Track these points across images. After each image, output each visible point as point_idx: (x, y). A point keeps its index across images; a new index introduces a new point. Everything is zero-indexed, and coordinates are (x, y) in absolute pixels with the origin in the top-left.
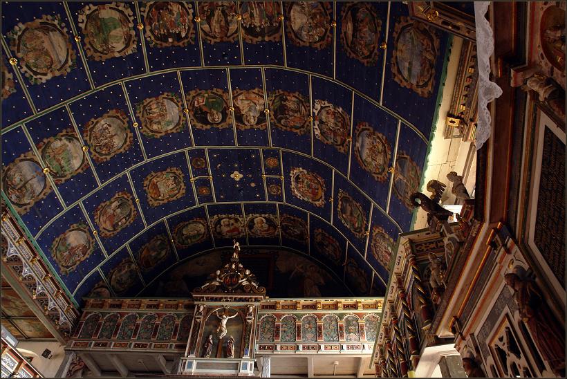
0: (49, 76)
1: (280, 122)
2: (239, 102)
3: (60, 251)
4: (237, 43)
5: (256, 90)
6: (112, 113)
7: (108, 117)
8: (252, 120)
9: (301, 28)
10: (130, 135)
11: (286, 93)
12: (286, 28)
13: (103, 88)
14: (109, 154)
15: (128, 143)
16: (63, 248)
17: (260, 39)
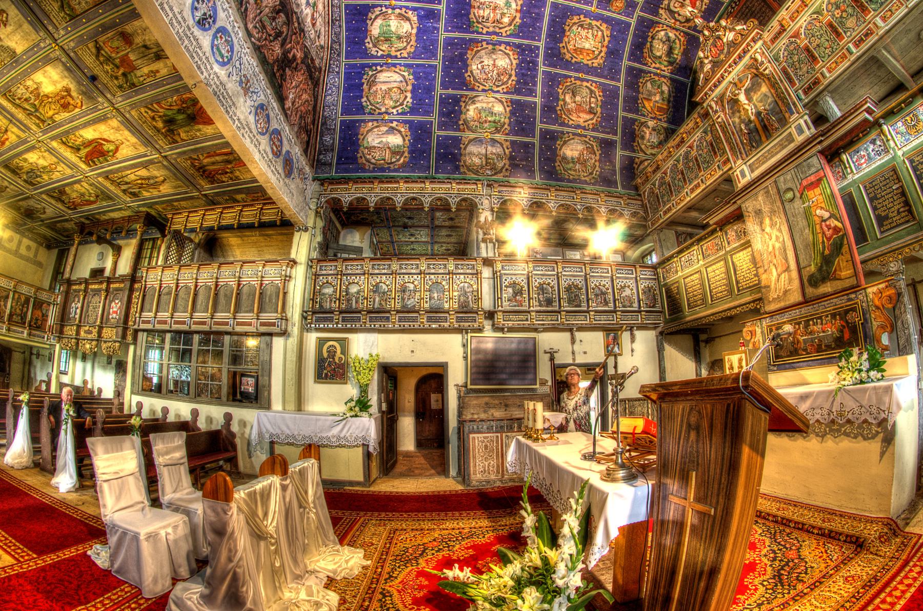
0: (409, 95)
6: (470, 54)
7: (472, 59)
10: (502, 47)
13: (440, 53)
14: (510, 76)
15: (511, 53)
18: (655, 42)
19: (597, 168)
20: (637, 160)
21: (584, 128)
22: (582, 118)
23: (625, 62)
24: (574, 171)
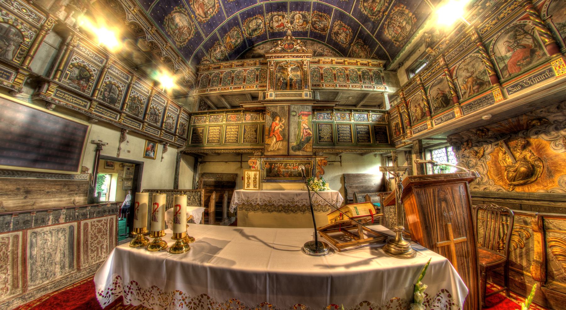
3: (172, 29)
16: (173, 27)
18: (255, 21)
19: (185, 43)
20: (205, 57)
21: (196, 17)
22: (199, 12)
23: (237, 13)
24: (173, 32)
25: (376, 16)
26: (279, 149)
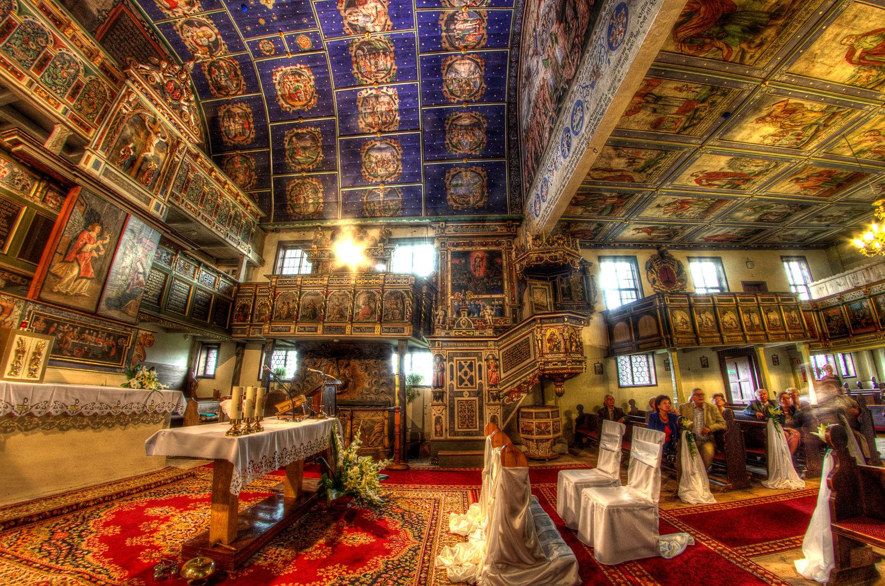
1: (359, 48)
2: (373, 4)
4: (440, 6)
5: (389, 22)
8: (352, 18)
9: (457, 72)
11: (392, 55)
12: (456, 55)
17: (444, 28)
25: (293, 162)
26: (78, 295)
